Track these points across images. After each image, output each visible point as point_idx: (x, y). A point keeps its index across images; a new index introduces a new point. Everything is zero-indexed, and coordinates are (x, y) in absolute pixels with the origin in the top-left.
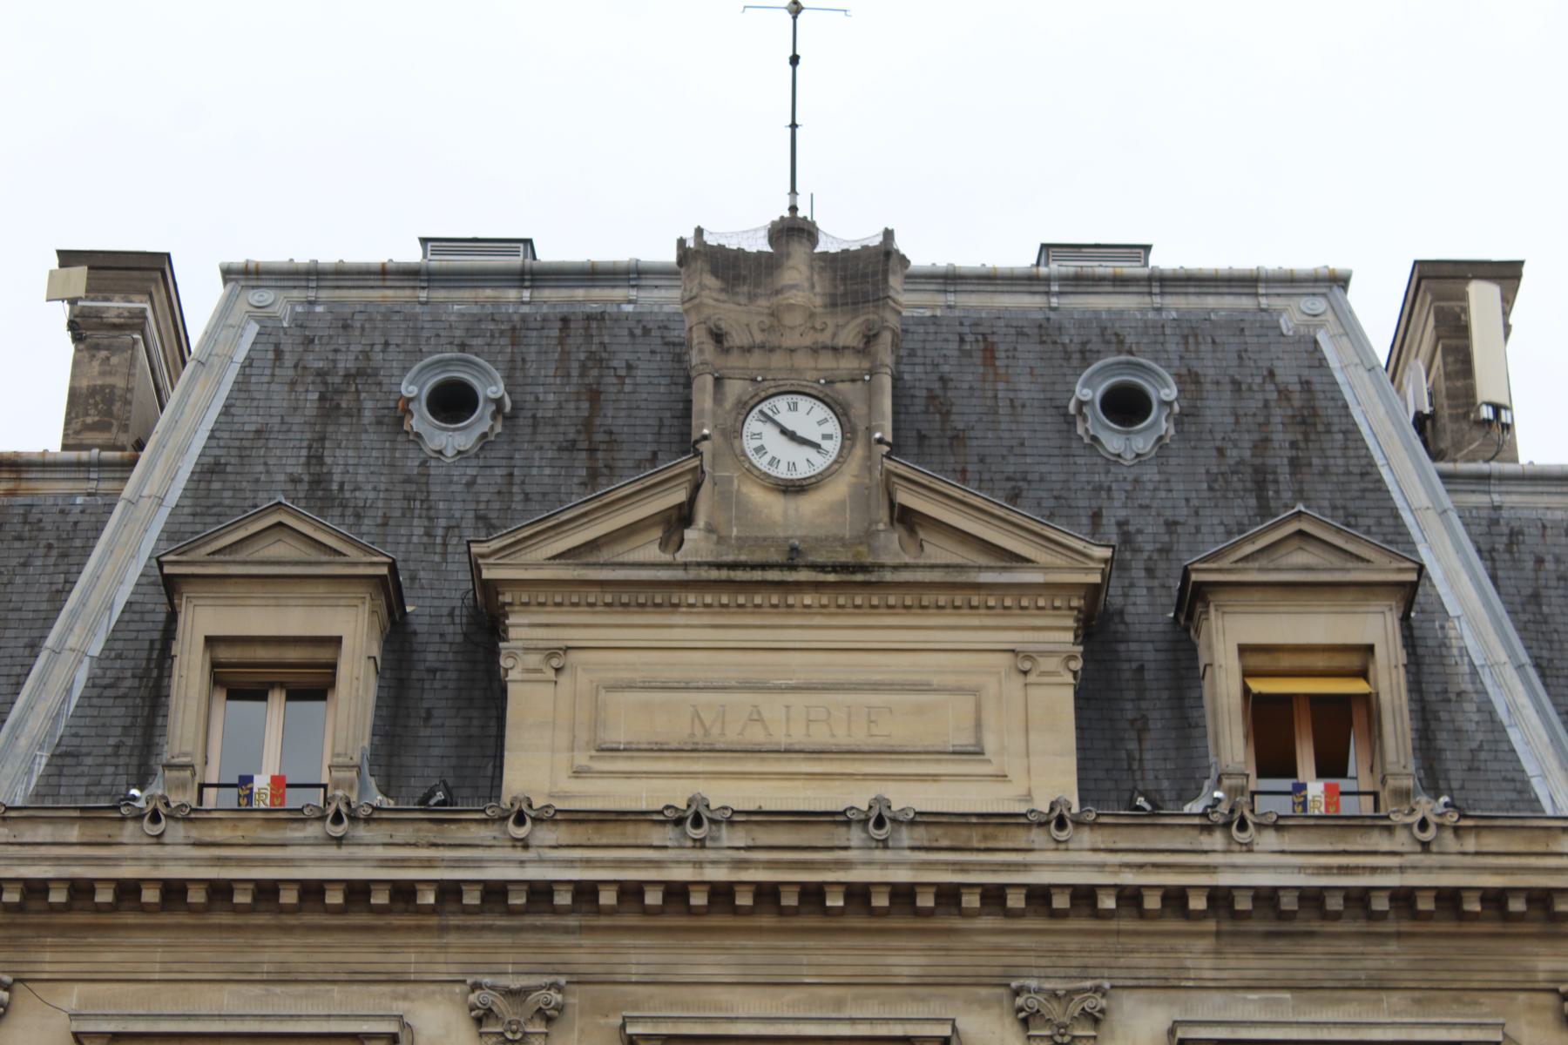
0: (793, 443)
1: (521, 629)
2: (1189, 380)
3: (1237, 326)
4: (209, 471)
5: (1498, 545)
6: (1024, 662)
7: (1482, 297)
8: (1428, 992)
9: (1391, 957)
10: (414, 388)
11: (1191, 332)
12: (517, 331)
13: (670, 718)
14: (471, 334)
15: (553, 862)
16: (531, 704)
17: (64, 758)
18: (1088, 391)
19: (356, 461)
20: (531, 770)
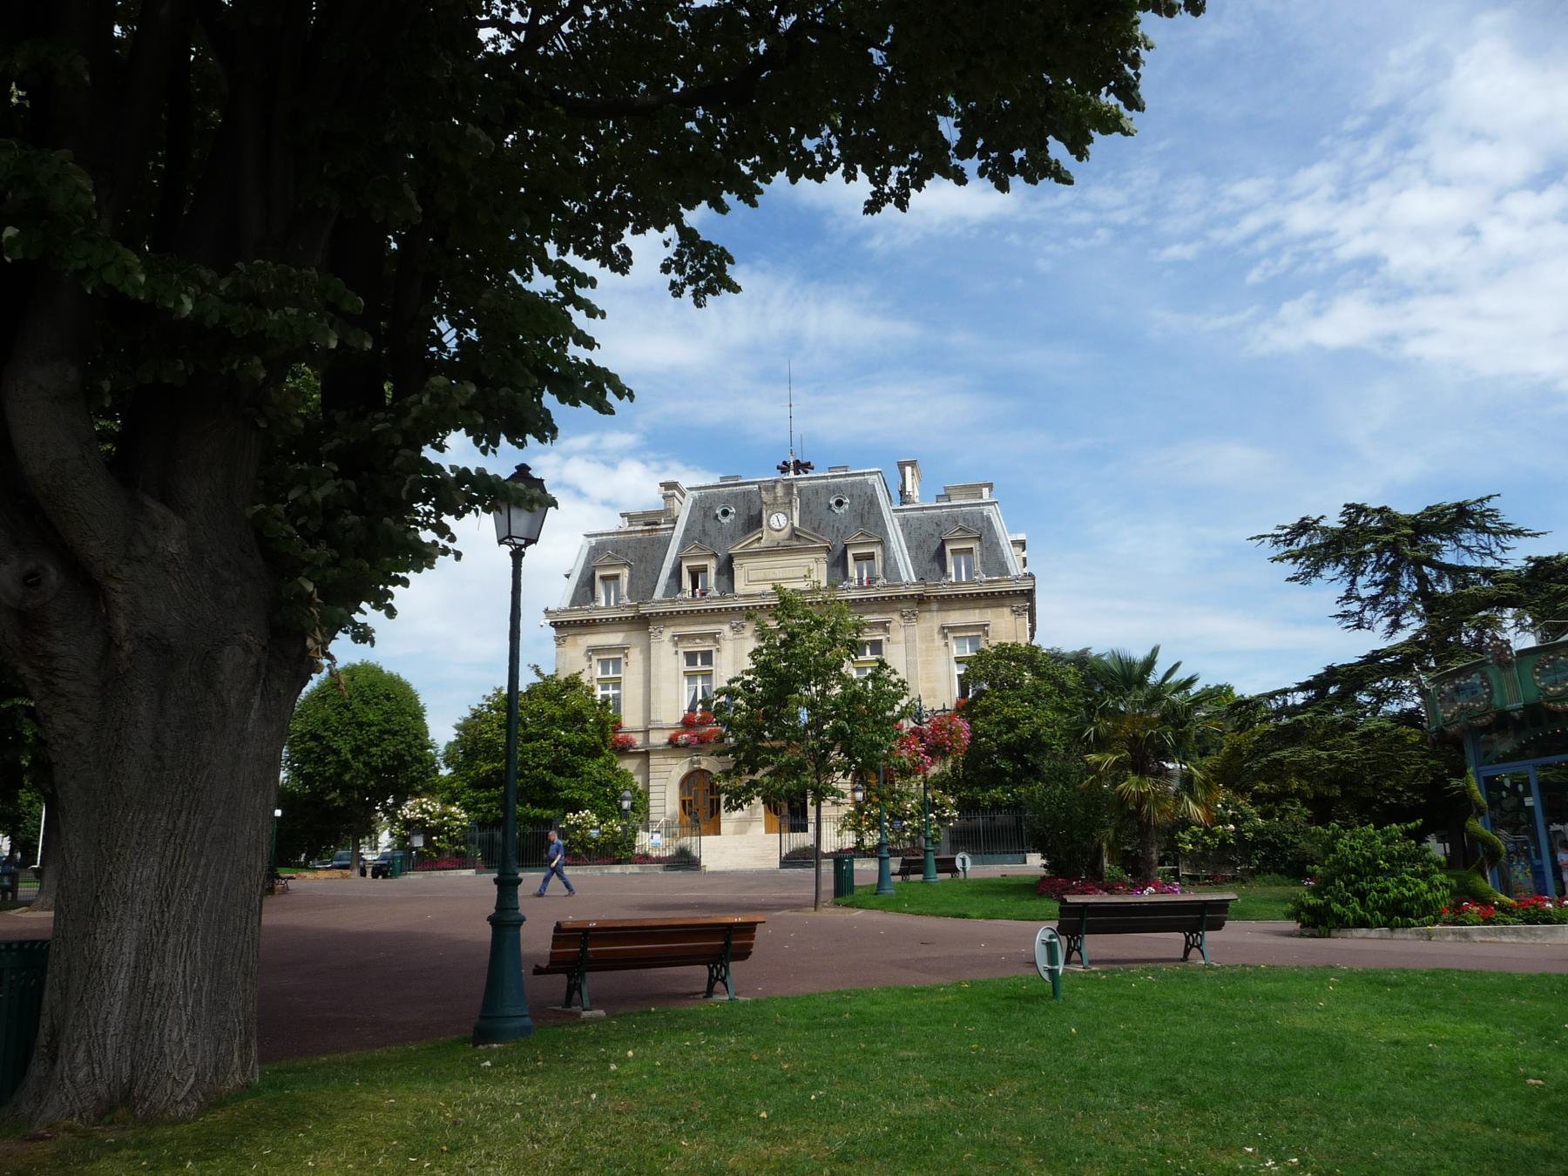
0: (778, 522)
1: (736, 562)
2: (851, 496)
3: (861, 482)
4: (686, 530)
5: (905, 524)
6: (817, 560)
7: (908, 469)
8: (881, 612)
9: (875, 607)
10: (718, 512)
11: (853, 484)
12: (736, 495)
13: (760, 575)
14: (727, 501)
15: (742, 603)
16: (739, 574)
17: (668, 587)
18: (832, 502)
19: (711, 526)
20: (740, 586)
